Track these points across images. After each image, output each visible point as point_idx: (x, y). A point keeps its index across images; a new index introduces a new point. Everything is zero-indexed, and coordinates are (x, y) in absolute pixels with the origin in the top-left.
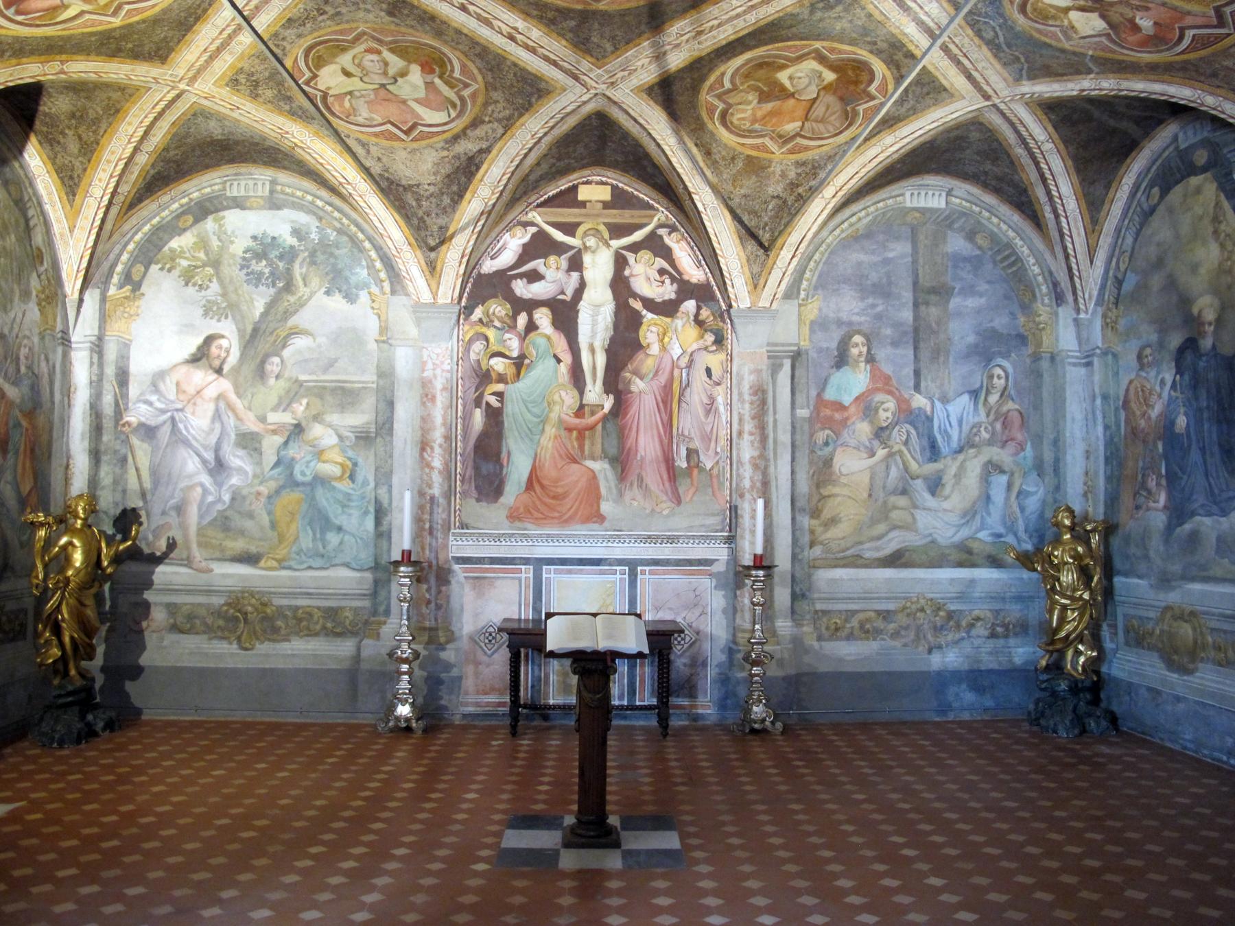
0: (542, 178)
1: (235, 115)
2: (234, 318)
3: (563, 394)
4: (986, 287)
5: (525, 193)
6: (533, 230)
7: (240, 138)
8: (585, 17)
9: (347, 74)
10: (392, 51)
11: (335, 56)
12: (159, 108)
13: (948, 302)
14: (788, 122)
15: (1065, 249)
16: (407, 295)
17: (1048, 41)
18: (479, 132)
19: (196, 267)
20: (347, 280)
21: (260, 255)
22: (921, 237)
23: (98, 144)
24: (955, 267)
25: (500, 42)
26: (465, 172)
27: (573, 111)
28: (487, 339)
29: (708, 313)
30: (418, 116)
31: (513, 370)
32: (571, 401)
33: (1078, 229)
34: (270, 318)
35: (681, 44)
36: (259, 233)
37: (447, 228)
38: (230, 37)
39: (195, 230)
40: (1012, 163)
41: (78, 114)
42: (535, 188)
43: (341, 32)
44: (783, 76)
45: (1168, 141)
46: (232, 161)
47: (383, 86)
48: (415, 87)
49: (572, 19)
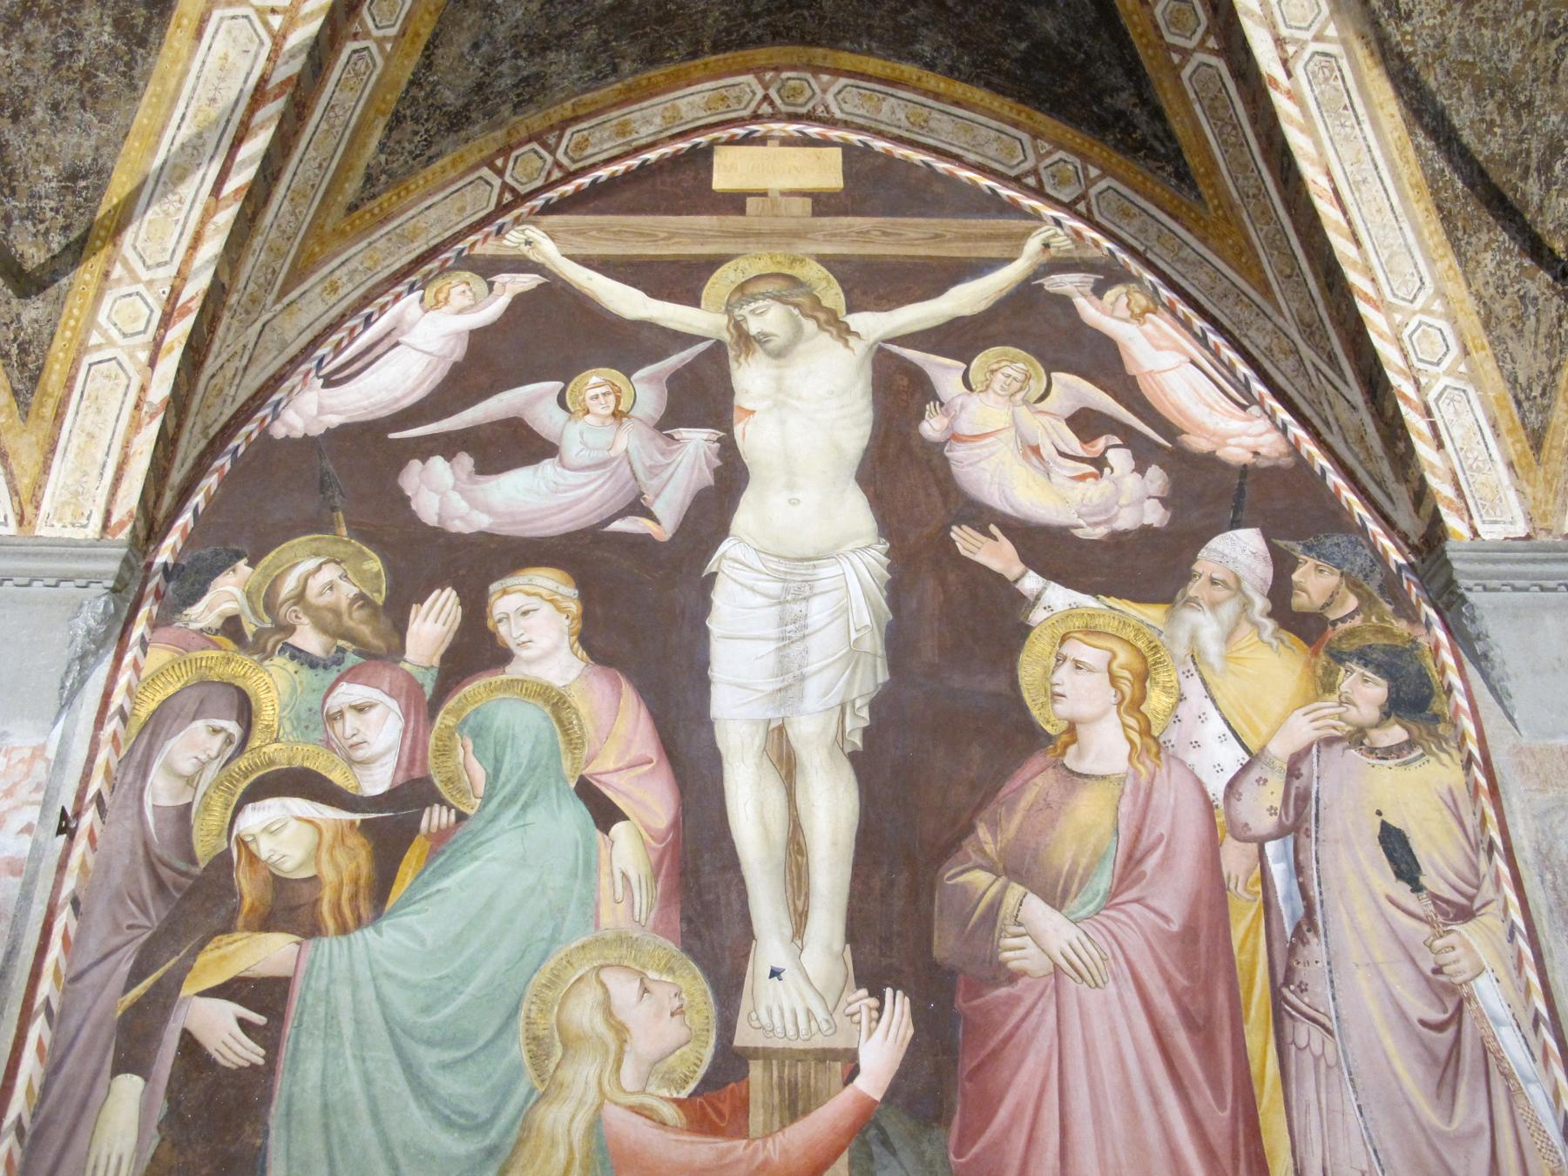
3: (623, 989)
6: (527, 282)
28: (245, 709)
29: (1330, 579)
31: (356, 860)
32: (672, 1030)
37: (101, 173)
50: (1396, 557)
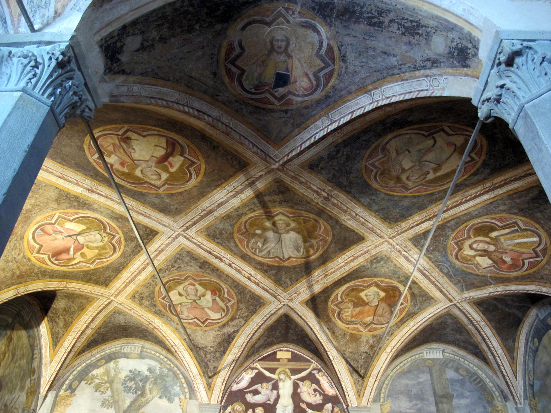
0: (260, 347)
1: (131, 313)
2: (115, 408)
4: (469, 393)
5: (253, 354)
6: (256, 371)
7: (131, 324)
8: (279, 269)
9: (180, 295)
10: (200, 284)
11: (176, 286)
12: (100, 308)
13: (452, 401)
14: (367, 317)
15: (502, 372)
16: (197, 400)
17: (470, 271)
18: (234, 323)
19: (102, 383)
20: (170, 392)
21: (131, 379)
22: (434, 372)
23: (72, 323)
24: (452, 385)
25: (244, 280)
26: (227, 341)
27: (275, 313)
30: (208, 315)
33: (505, 362)
34: (132, 408)
35: (319, 280)
36: (133, 369)
37: (217, 367)
38: (135, 276)
39: (105, 367)
40: (468, 333)
41: (67, 309)
42: (257, 352)
43: (180, 276)
44: (363, 295)
45: (535, 317)
46: (126, 336)
47: (195, 301)
48: (208, 302)
49: (274, 270)
50: (345, 407)
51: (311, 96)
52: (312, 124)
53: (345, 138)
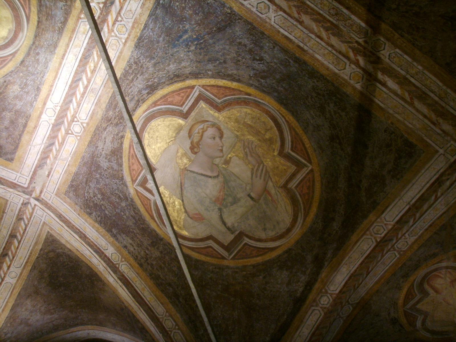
51: (429, 271)
52: (422, 234)
53: (366, 222)
